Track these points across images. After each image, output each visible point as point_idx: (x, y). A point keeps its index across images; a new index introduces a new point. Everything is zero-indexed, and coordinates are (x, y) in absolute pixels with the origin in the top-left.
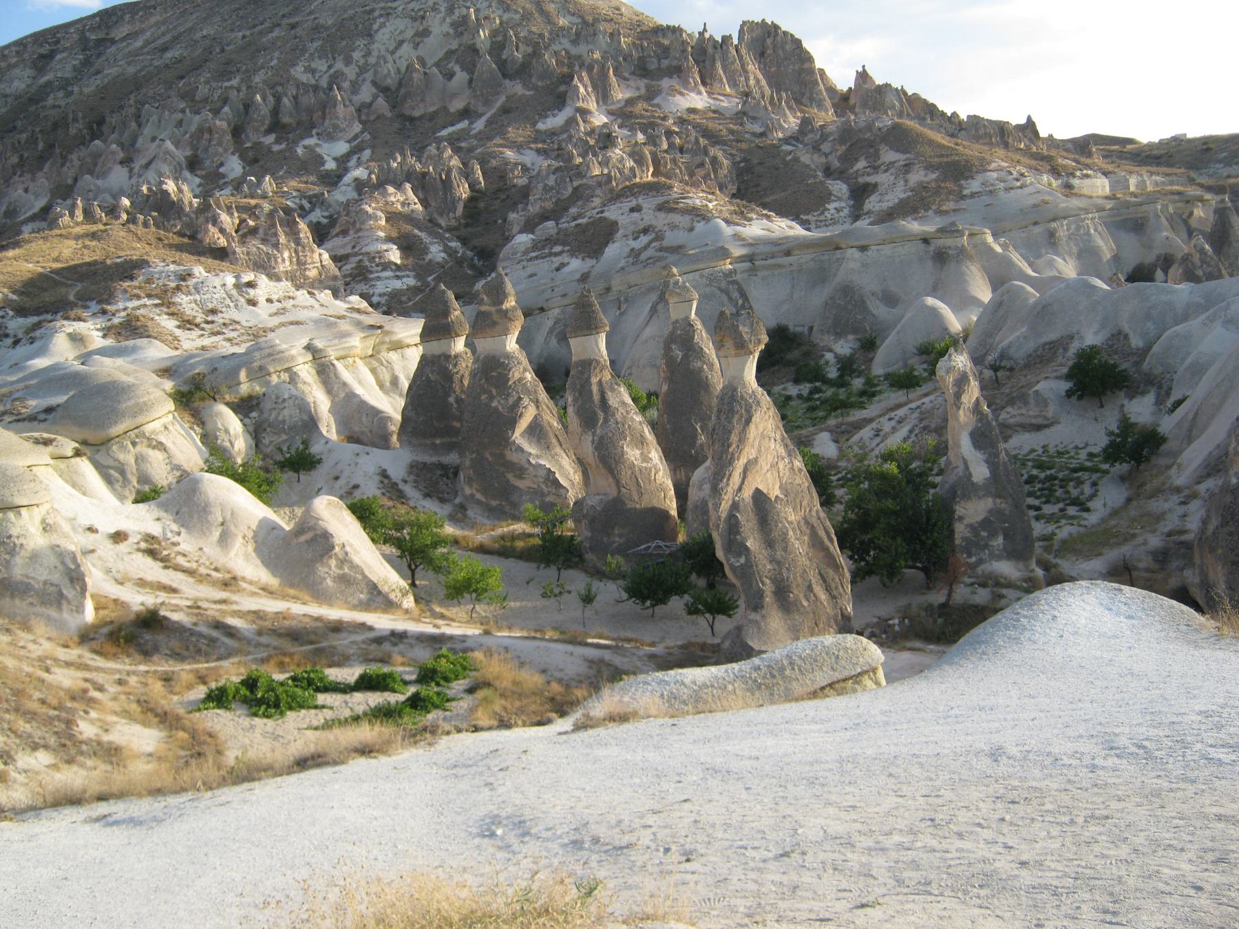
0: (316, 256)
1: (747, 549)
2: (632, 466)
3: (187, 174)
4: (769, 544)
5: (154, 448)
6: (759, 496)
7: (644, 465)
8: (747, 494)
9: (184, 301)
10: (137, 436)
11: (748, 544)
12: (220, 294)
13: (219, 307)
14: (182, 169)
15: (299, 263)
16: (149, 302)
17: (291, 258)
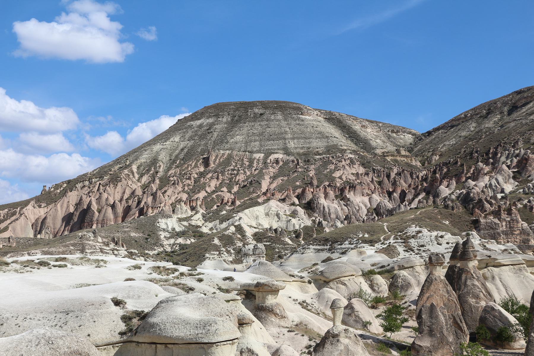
0: (520, 225)
1: (422, 317)
2: (470, 305)
3: (512, 181)
4: (431, 317)
5: (343, 285)
6: (432, 305)
7: (477, 305)
8: (428, 305)
9: (413, 242)
10: (338, 281)
11: (423, 316)
12: (428, 239)
13: (425, 244)
14: (509, 178)
15: (510, 227)
16: (400, 241)
17: (506, 225)
